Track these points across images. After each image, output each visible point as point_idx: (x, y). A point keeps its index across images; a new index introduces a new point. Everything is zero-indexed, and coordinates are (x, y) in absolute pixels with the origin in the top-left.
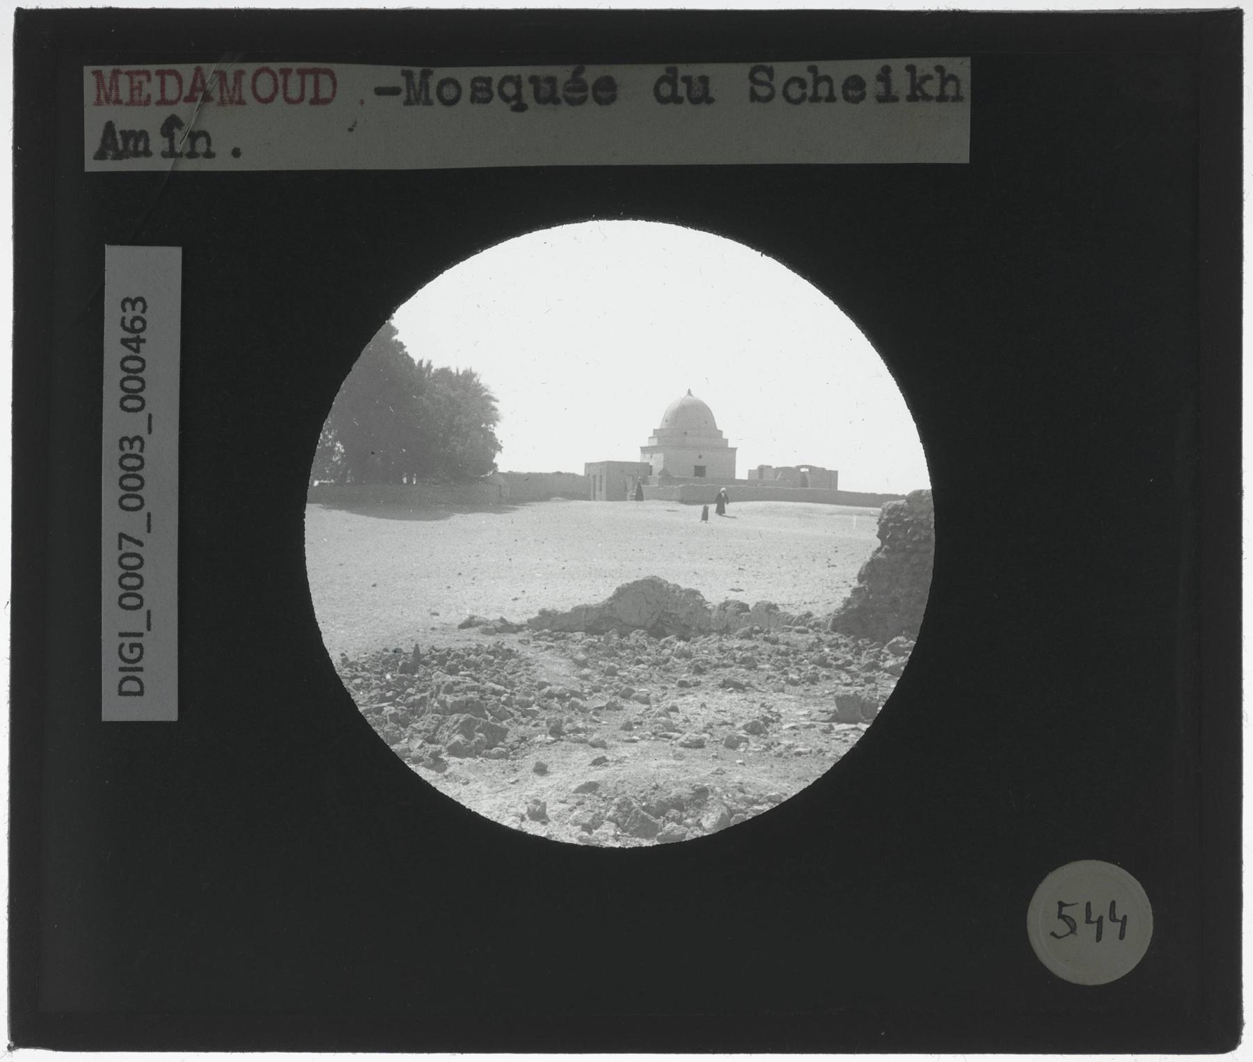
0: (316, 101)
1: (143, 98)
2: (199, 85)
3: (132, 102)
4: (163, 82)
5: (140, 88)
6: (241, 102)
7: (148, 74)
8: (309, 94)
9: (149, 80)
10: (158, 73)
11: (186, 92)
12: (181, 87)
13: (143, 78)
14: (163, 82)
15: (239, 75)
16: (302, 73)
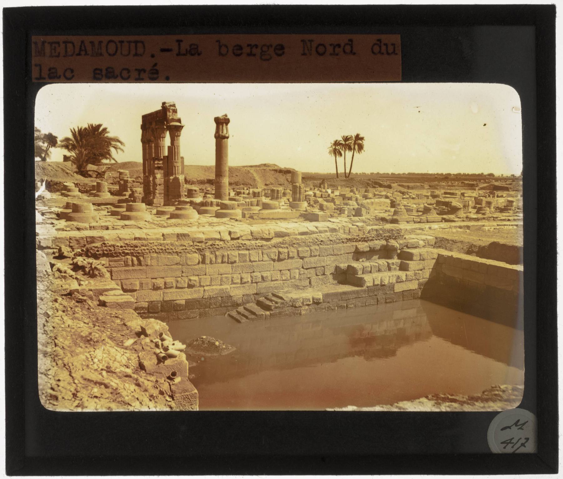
0: (136, 55)
1: (57, 54)
2: (83, 48)
3: (51, 56)
4: (66, 45)
5: (55, 49)
6: (101, 55)
7: (58, 43)
8: (133, 52)
9: (59, 46)
10: (64, 42)
11: (77, 51)
12: (74, 49)
13: (57, 45)
14: (66, 48)
15: (100, 42)
16: (129, 42)
